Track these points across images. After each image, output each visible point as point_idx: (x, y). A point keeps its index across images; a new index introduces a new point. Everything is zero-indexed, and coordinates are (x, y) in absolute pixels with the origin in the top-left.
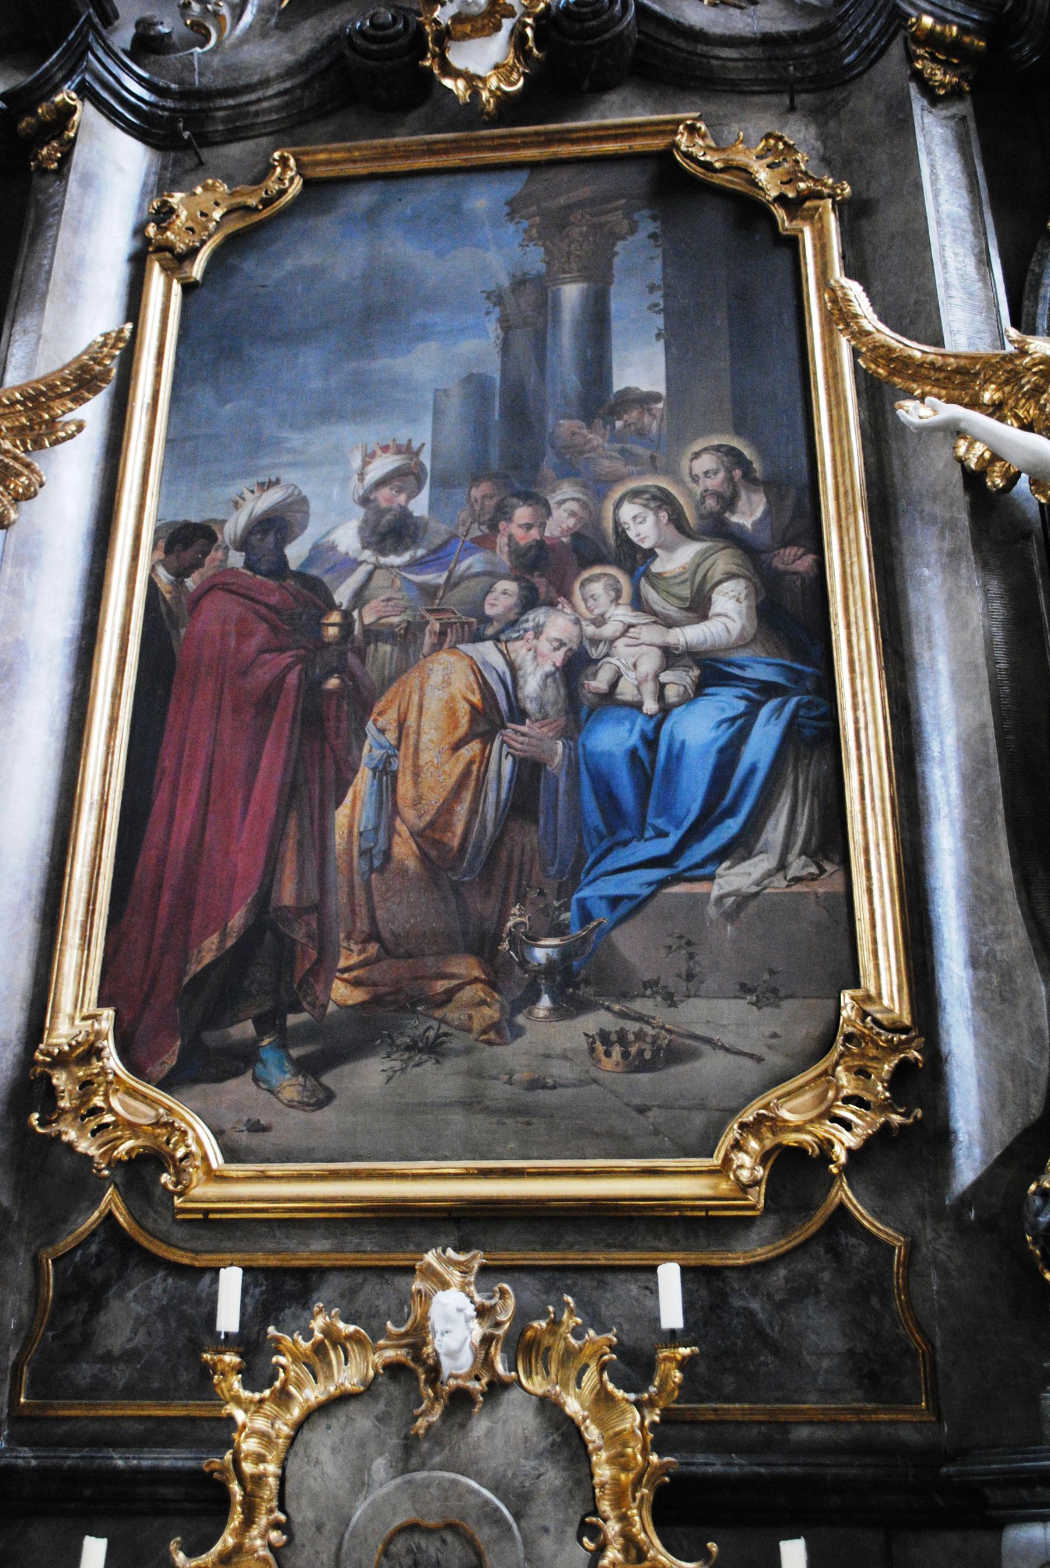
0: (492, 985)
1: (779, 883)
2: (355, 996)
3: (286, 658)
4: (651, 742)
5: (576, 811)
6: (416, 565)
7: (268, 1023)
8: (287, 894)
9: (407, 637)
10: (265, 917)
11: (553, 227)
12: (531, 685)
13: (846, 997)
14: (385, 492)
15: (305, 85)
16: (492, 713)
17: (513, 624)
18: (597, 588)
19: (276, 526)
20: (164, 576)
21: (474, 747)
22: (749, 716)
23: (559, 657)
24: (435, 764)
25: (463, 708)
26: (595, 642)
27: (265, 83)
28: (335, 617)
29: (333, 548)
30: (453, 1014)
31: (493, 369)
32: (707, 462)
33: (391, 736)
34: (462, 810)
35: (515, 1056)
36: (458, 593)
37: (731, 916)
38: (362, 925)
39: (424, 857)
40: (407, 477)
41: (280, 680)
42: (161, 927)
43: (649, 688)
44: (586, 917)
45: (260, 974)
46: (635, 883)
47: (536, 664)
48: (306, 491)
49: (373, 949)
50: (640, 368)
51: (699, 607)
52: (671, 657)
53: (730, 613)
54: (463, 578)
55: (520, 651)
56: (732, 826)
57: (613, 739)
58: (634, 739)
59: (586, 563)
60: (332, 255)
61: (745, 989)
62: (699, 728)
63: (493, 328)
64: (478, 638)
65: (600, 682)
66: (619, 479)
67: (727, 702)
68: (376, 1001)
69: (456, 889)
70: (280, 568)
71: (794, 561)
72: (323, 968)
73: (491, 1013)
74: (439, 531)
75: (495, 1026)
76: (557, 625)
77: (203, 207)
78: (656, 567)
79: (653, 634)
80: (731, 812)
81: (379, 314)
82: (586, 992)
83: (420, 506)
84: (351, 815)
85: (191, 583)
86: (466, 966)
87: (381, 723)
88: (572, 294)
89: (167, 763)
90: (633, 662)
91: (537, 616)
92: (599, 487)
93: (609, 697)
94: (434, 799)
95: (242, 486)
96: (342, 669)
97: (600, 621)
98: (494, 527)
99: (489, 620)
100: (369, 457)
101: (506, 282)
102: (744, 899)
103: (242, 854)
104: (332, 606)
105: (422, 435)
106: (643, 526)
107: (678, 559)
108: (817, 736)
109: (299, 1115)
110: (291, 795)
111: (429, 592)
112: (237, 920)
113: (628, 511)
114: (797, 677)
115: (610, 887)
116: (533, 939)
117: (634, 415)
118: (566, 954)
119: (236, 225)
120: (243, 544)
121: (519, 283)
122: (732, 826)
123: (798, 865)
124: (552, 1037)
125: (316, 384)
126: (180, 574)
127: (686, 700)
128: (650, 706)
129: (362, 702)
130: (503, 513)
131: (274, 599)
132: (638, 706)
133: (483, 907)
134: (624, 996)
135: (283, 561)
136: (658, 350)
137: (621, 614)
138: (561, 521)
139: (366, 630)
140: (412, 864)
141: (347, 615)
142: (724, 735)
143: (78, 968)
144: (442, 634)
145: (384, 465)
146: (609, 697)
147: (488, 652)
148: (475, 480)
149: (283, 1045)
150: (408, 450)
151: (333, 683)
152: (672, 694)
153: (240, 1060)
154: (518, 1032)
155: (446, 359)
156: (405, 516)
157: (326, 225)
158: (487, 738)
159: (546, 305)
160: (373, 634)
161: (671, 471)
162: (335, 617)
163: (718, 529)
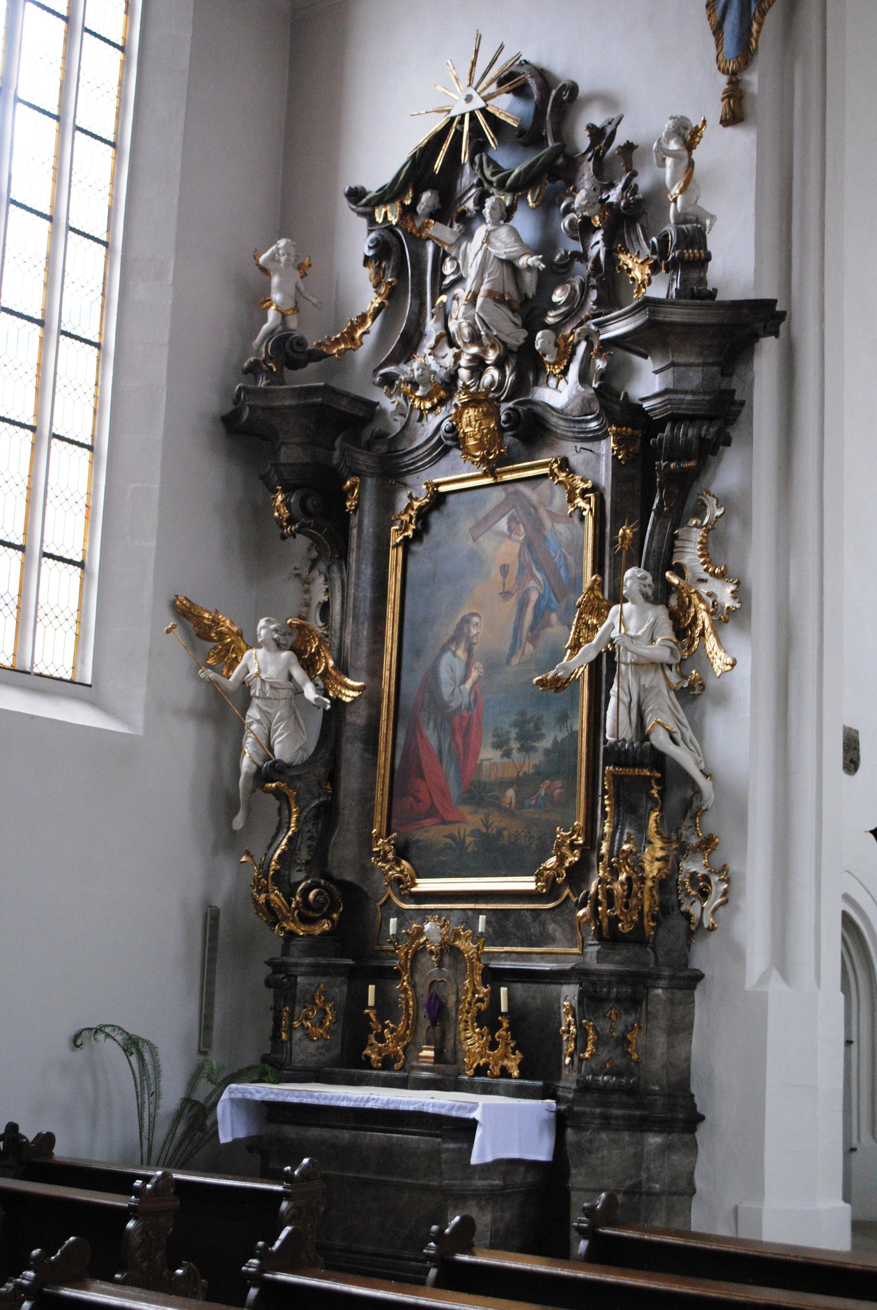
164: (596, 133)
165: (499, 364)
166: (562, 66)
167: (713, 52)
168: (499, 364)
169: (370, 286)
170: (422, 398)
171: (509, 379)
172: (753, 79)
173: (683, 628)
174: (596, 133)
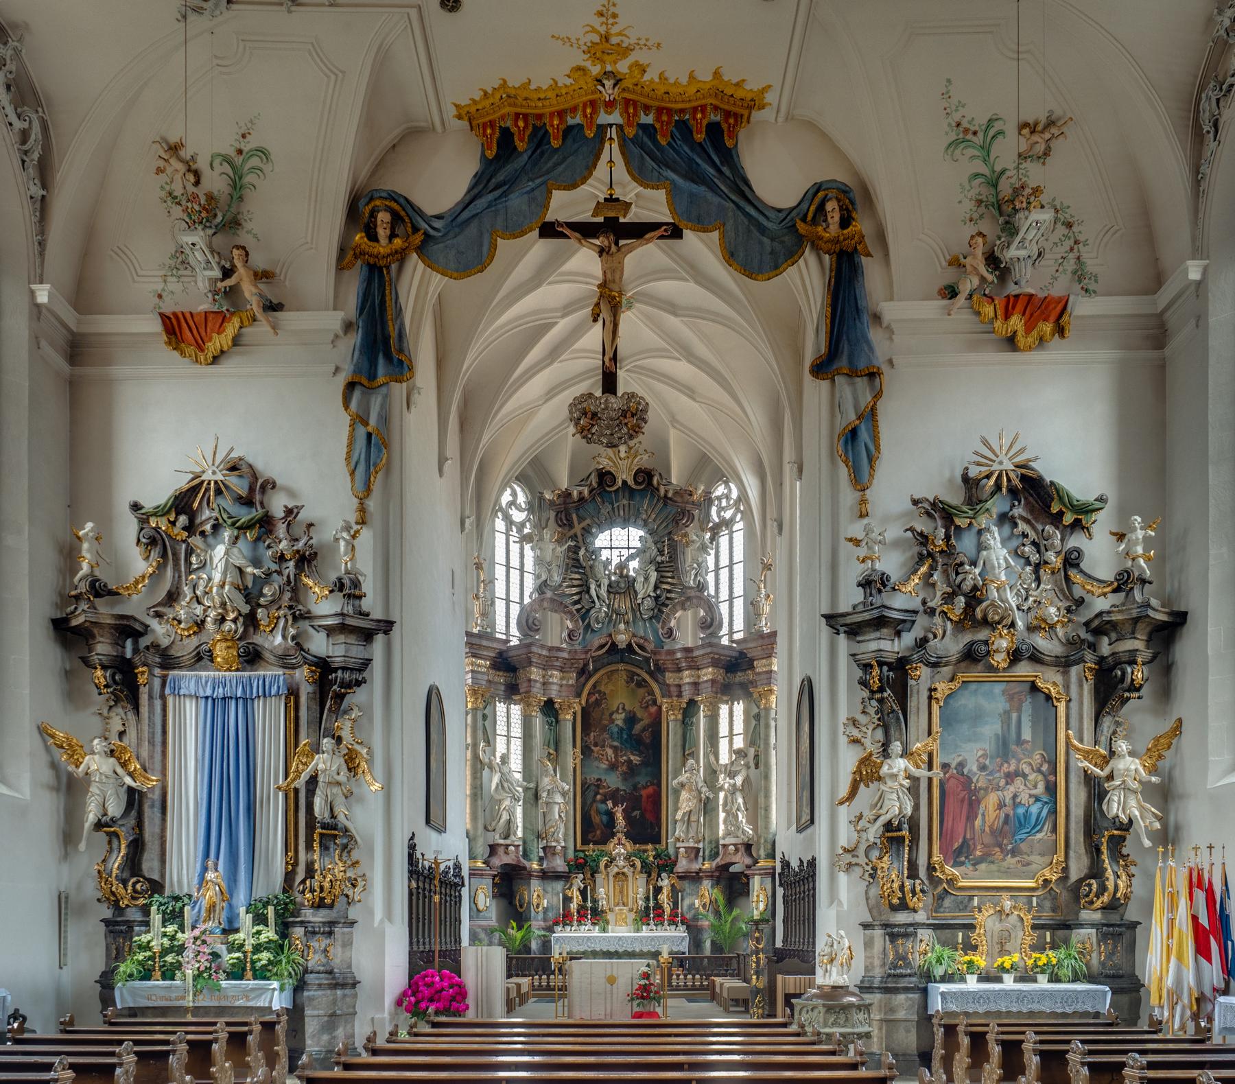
9: (986, 789)
16: (1001, 806)
19: (961, 765)
40: (984, 756)
47: (1008, 795)
50: (1027, 735)
51: (1035, 787)
52: (1031, 796)
60: (967, 701)
70: (963, 774)
71: (1052, 778)
72: (975, 848)
74: (991, 768)
76: (1012, 789)
81: (977, 717)
83: (987, 762)
87: (982, 806)
90: (1024, 798)
92: (1019, 761)
105: (987, 747)
106: (1027, 770)
107: (1032, 777)
110: (968, 818)
129: (979, 802)
130: (1002, 765)
137: (1022, 787)
138: (1012, 768)
145: (980, 753)
155: (991, 729)
163: (1039, 771)
164: (289, 511)
165: (235, 621)
166: (267, 466)
167: (349, 485)
168: (235, 621)
169: (140, 558)
170: (183, 629)
171: (241, 630)
172: (371, 504)
173: (352, 768)
174: (289, 511)
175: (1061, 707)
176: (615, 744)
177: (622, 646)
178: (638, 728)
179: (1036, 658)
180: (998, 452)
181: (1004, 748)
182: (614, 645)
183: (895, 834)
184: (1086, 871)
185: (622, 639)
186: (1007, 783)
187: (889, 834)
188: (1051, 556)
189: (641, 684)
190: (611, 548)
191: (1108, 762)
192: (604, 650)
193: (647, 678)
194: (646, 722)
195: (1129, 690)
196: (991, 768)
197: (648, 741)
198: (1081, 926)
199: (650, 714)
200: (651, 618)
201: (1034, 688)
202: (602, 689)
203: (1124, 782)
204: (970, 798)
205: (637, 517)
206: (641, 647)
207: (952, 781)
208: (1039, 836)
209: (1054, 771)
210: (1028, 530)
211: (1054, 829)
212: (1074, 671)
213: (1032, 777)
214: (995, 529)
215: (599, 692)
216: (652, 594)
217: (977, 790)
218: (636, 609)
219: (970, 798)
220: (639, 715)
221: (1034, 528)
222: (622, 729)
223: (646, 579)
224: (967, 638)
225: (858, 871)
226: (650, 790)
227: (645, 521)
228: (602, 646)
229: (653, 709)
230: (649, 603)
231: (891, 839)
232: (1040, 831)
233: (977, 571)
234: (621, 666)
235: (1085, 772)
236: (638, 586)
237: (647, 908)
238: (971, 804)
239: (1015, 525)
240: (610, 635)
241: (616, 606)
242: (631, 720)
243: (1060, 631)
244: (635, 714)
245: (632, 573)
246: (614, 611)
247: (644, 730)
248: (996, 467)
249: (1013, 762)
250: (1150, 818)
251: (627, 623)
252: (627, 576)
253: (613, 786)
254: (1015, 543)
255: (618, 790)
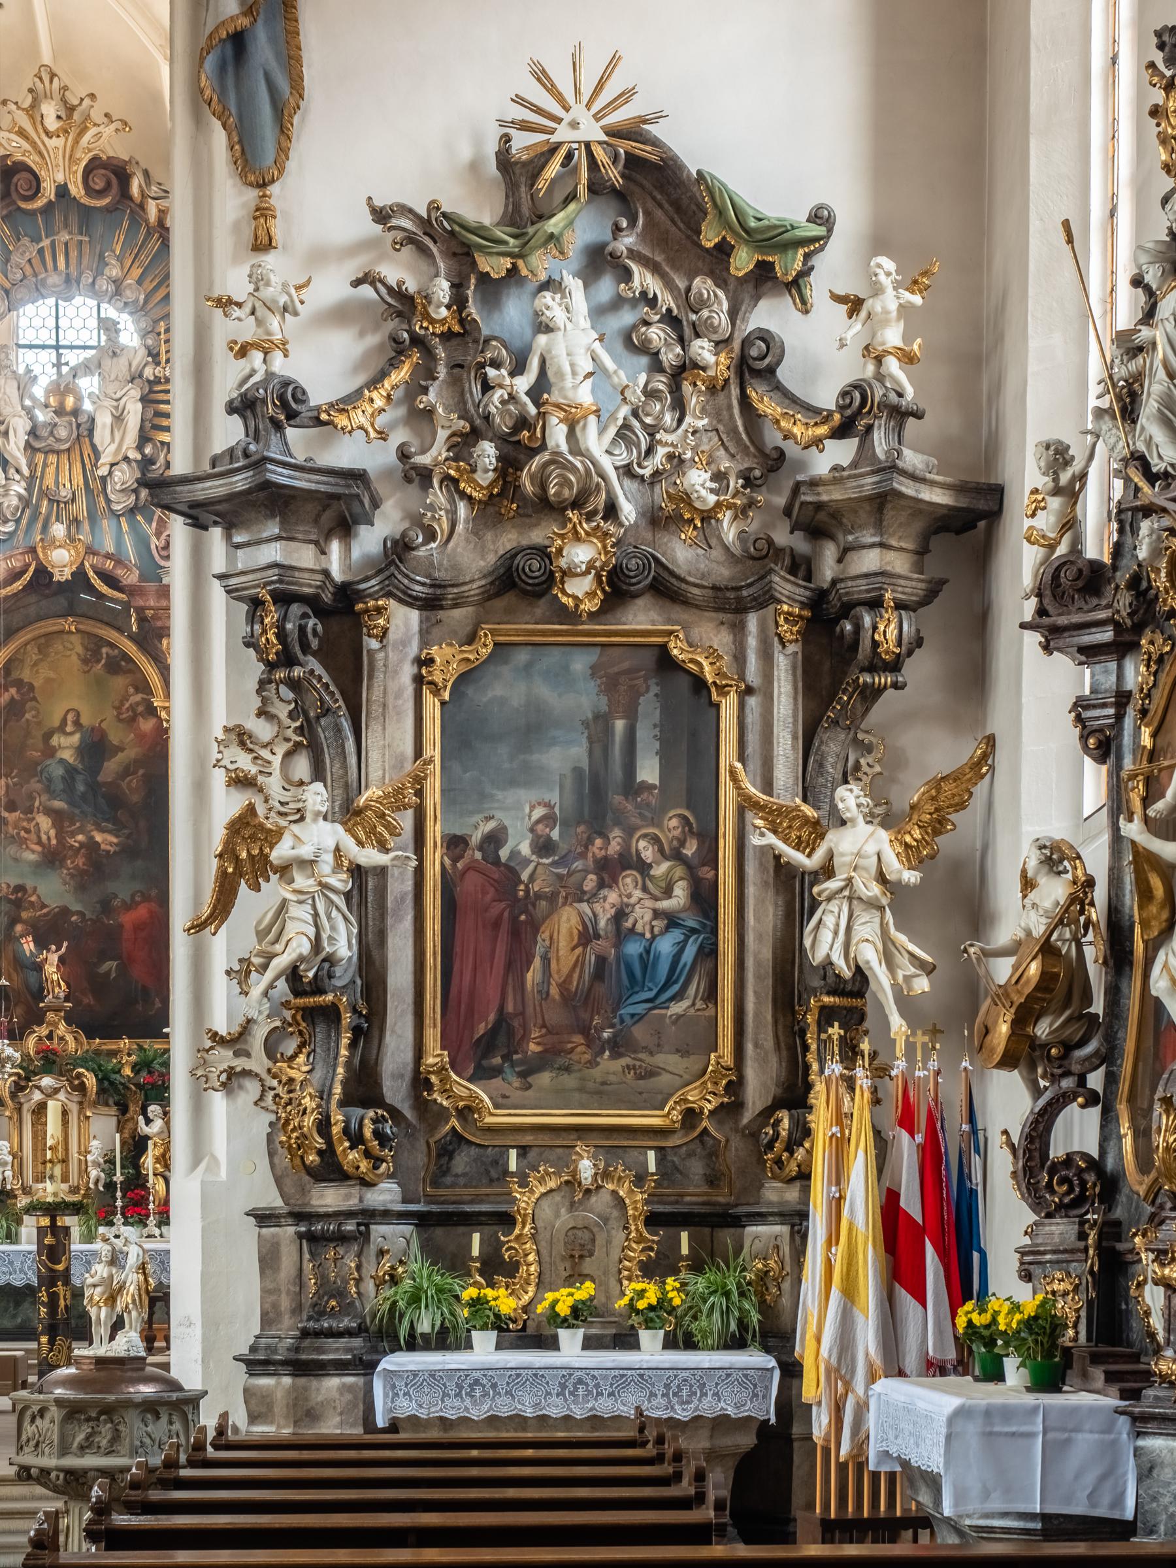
0: (588, 1046)
1: (692, 1011)
2: (538, 1049)
3: (503, 905)
4: (648, 951)
5: (619, 980)
6: (554, 864)
7: (506, 1057)
8: (510, 1008)
9: (552, 898)
10: (502, 1018)
11: (610, 685)
12: (602, 923)
13: (712, 1056)
14: (540, 827)
15: (492, 583)
16: (587, 935)
17: (595, 895)
18: (628, 880)
19: (494, 840)
20: (447, 861)
21: (579, 950)
22: (685, 941)
23: (613, 911)
24: (565, 956)
25: (575, 932)
26: (627, 905)
27: (472, 581)
28: (522, 887)
29: (519, 853)
30: (574, 1056)
31: (585, 764)
32: (674, 822)
33: (547, 943)
34: (576, 976)
35: (597, 1073)
36: (572, 880)
37: (675, 1023)
38: (540, 1021)
39: (561, 994)
41: (501, 914)
42: (462, 1019)
43: (648, 927)
44: (622, 1021)
45: (502, 1039)
46: (640, 1009)
48: (506, 823)
49: (544, 1031)
50: (649, 771)
51: (668, 893)
52: (657, 914)
53: (680, 895)
54: (575, 872)
55: (598, 907)
56: (676, 987)
57: (633, 949)
58: (641, 949)
59: (624, 868)
61: (678, 1051)
62: (666, 946)
63: (584, 741)
64: (581, 901)
65: (629, 924)
66: (638, 828)
67: (676, 935)
68: (545, 1051)
69: (575, 1007)
70: (497, 862)
71: (706, 873)
73: (588, 1057)
74: (563, 848)
75: (589, 1062)
76: (613, 897)
77: (448, 659)
78: (652, 872)
79: (649, 903)
80: (676, 982)
81: (533, 729)
82: (622, 1050)
83: (555, 834)
84: (533, 976)
85: (460, 865)
86: (578, 1039)
87: (543, 936)
88: (620, 725)
89: (457, 949)
90: (642, 917)
91: (604, 892)
92: (630, 832)
93: (632, 930)
94: (565, 971)
95: (477, 818)
96: (526, 912)
97: (629, 896)
98: (586, 848)
99: (584, 892)
100: (532, 808)
101: (590, 716)
102: (679, 1017)
103: (491, 992)
104: (521, 882)
106: (648, 852)
107: (661, 869)
108: (709, 952)
109: (519, 1093)
110: (509, 966)
111: (560, 877)
112: (492, 1017)
113: (642, 844)
114: (704, 925)
115: (631, 1010)
116: (603, 1029)
117: (645, 795)
118: (615, 1035)
119: (464, 668)
120: (480, 848)
121: (597, 717)
122: (676, 987)
123: (699, 1004)
124: (609, 1066)
125: (507, 765)
126: (455, 860)
127: (662, 933)
128: (648, 936)
130: (590, 841)
131: (496, 876)
132: (643, 935)
133: (585, 1016)
134: (635, 1052)
135: (498, 857)
136: (656, 761)
137: (638, 893)
138: (614, 847)
139: (535, 893)
140: (557, 997)
141: (527, 886)
142: (676, 949)
143: (432, 1036)
144: (566, 898)
145: (538, 813)
146: (632, 930)
147: (584, 907)
148: (578, 823)
149: (512, 1066)
150: (548, 805)
151: (523, 917)
152: (656, 930)
153: (496, 1072)
154: (598, 1064)
155: (565, 756)
156: (549, 838)
157: (505, 671)
158: (585, 945)
159: (608, 731)
160: (539, 896)
161: (659, 825)
162: (522, 887)
163: (677, 856)
175: (728, 707)
176: (58, 804)
177: (63, 575)
178: (111, 767)
179: (666, 588)
180: (570, 97)
181: (598, 799)
182: (43, 573)
183: (311, 1001)
184: (773, 1090)
185: (61, 561)
186: (601, 885)
187: (300, 1001)
188: (702, 349)
189: (119, 664)
190: (57, 347)
191: (822, 836)
192: (18, 585)
193: (131, 648)
194: (131, 753)
195: (871, 669)
196: (563, 848)
197: (135, 798)
198: (760, 1218)
199: (141, 736)
200: (132, 511)
201: (665, 662)
202: (26, 675)
203: (850, 880)
204: (514, 919)
205: (99, 273)
206: (110, 580)
207: (473, 879)
208: (677, 1008)
209: (711, 857)
210: (653, 285)
211: (711, 994)
212: (752, 621)
213: (661, 869)
214: (574, 285)
215: (19, 683)
216: (134, 455)
217: (532, 899)
218: (96, 488)
219: (514, 919)
220: (115, 736)
221: (669, 284)
222: (71, 771)
223: (119, 419)
224: (508, 540)
225: (252, 1089)
226: (142, 912)
227: (117, 283)
228: (16, 575)
229: (147, 725)
230: (125, 476)
231: (311, 1014)
232: (678, 997)
233: (523, 384)
234: (69, 624)
235: (777, 858)
236: (102, 436)
237: (110, 1186)
238: (516, 932)
239: (627, 276)
240: (33, 550)
241: (49, 480)
242: (95, 748)
243: (729, 529)
244: (103, 735)
245: (87, 406)
246: (44, 493)
247: (127, 771)
248: (563, 134)
249: (616, 834)
250: (906, 969)
251: (75, 522)
252: (76, 412)
253: (53, 903)
254: (627, 317)
255: (65, 912)
